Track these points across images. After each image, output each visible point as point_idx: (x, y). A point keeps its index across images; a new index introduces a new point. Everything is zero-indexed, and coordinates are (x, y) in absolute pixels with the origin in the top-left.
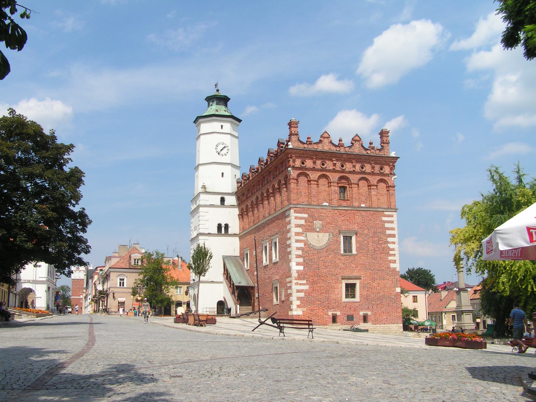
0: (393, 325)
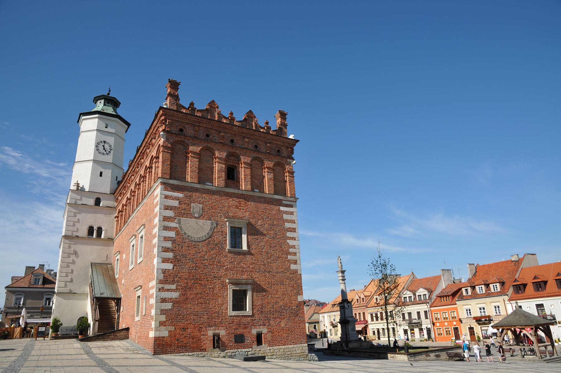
0: (295, 346)
